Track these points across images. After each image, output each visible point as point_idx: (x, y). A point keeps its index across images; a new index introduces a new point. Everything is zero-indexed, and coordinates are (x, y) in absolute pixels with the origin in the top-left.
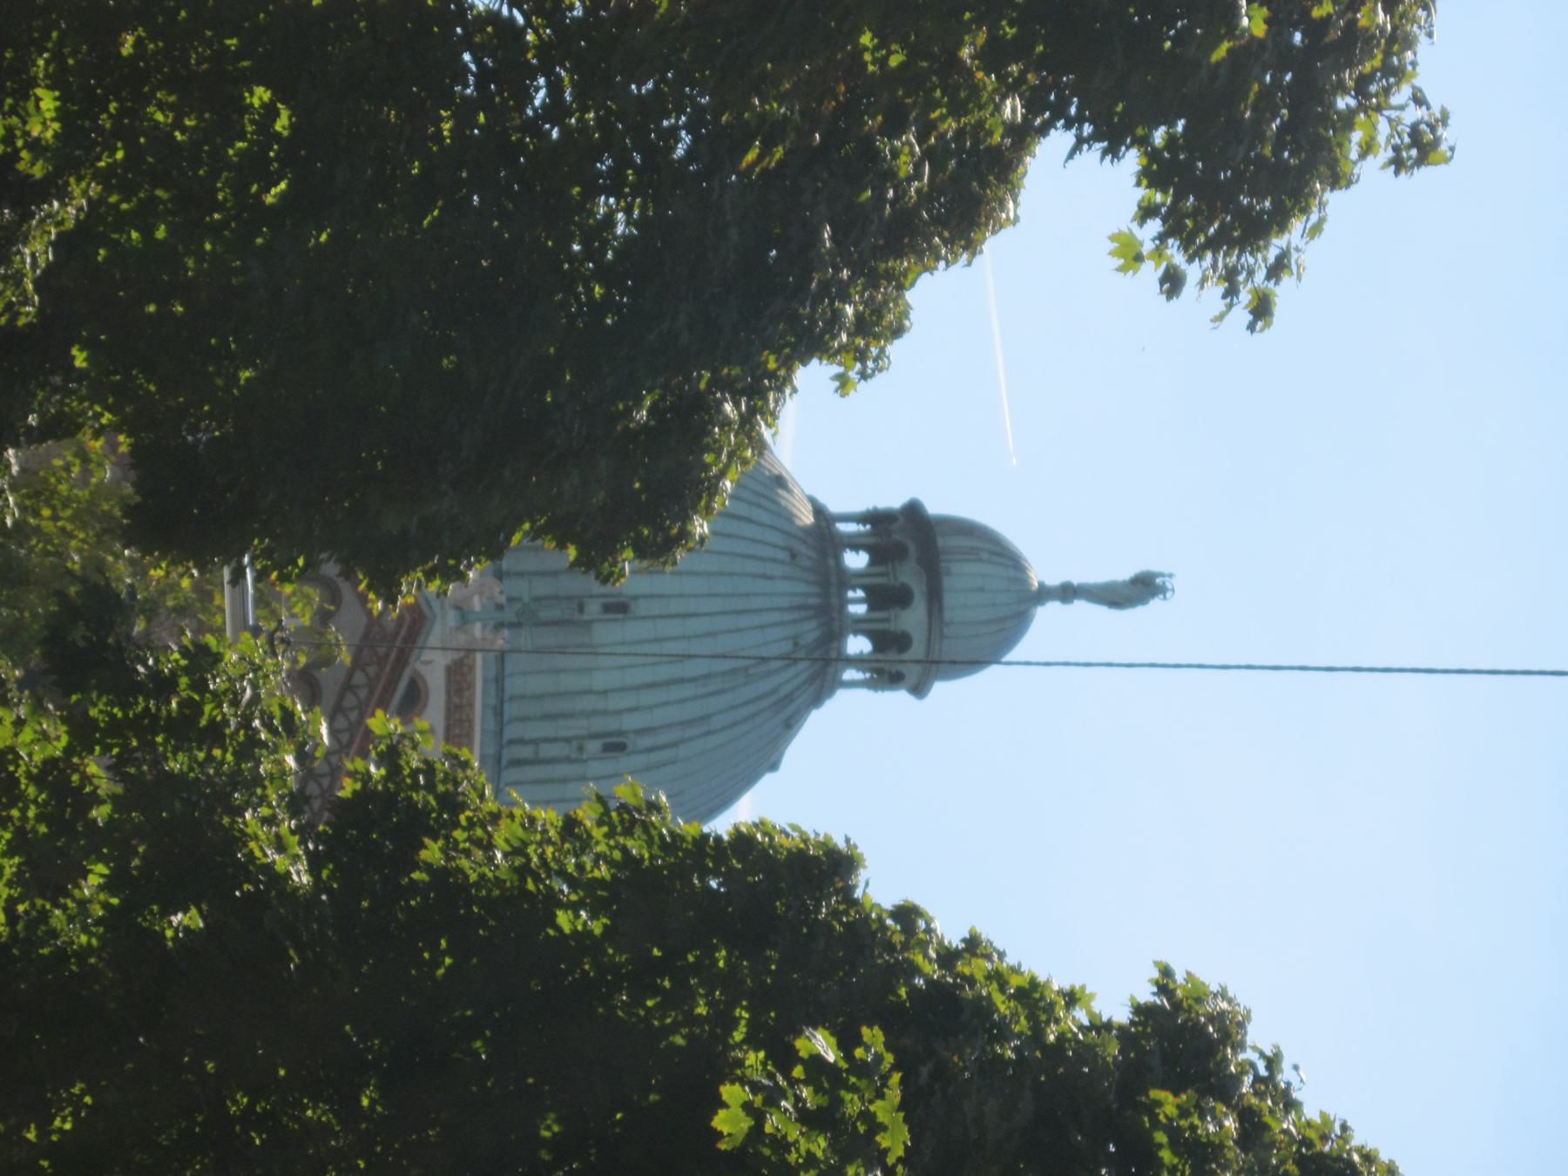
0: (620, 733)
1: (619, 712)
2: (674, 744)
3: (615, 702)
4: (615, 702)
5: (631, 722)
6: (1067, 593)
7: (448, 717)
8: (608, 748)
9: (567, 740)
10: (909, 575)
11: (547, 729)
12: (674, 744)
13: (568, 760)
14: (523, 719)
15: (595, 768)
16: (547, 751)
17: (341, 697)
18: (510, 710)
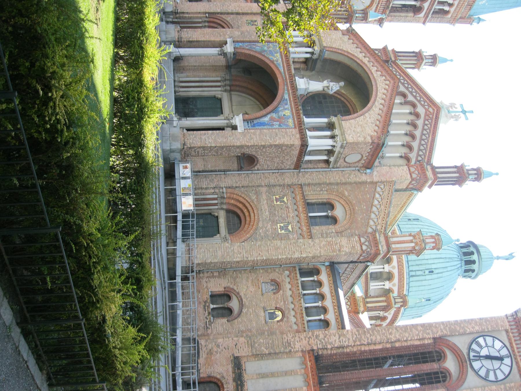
0: (432, 269)
1: (431, 264)
2: (442, 273)
3: (430, 262)
4: (430, 262)
5: (434, 266)
6: (498, 258)
7: (398, 264)
8: (430, 272)
9: (421, 270)
10: (472, 249)
11: (417, 268)
12: (442, 273)
13: (422, 275)
14: (412, 266)
15: (428, 277)
16: (418, 273)
17: (423, 127)
18: (410, 263)
